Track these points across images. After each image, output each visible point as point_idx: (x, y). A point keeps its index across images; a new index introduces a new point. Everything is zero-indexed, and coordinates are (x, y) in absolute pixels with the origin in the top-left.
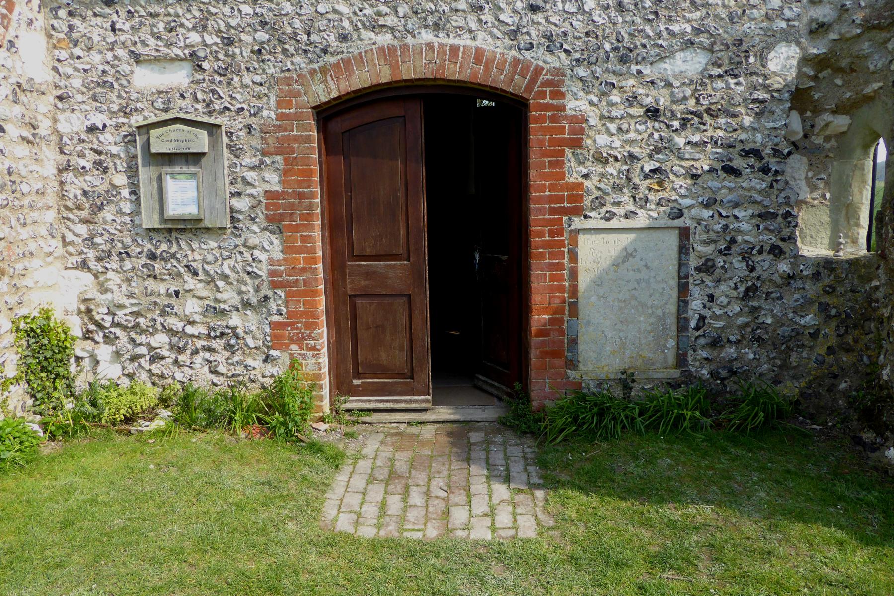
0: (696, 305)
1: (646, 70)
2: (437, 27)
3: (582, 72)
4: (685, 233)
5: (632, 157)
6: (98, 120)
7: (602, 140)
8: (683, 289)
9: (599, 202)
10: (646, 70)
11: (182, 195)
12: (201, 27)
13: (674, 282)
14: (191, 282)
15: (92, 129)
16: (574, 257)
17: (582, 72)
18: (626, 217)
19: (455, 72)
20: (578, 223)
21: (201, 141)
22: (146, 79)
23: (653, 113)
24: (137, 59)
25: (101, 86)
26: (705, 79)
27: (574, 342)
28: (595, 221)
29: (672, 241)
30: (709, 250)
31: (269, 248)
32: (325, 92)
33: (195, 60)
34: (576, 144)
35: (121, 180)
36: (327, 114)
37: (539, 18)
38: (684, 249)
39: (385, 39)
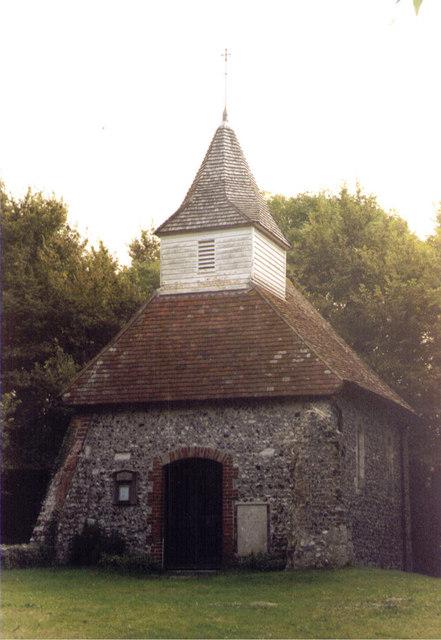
0: (272, 531)
1: (256, 454)
2: (199, 442)
3: (238, 455)
4: (268, 506)
5: (252, 482)
6: (103, 470)
7: (243, 476)
8: (269, 526)
9: (243, 496)
10: (256, 454)
11: (124, 493)
12: (134, 442)
13: (265, 523)
14: (124, 522)
15: (102, 474)
16: (236, 513)
17: (238, 455)
18: (251, 500)
19: (201, 455)
20: (237, 503)
21: (128, 477)
22: (119, 457)
23: (258, 468)
24: (116, 452)
25: (104, 462)
26: (272, 459)
27: (236, 543)
28: (241, 502)
29: (265, 508)
30: (275, 512)
31: (148, 511)
32: (167, 461)
33: (131, 452)
34: (236, 478)
35: (108, 489)
36: (166, 467)
37: (226, 439)
38: (268, 512)
39: (184, 445)
